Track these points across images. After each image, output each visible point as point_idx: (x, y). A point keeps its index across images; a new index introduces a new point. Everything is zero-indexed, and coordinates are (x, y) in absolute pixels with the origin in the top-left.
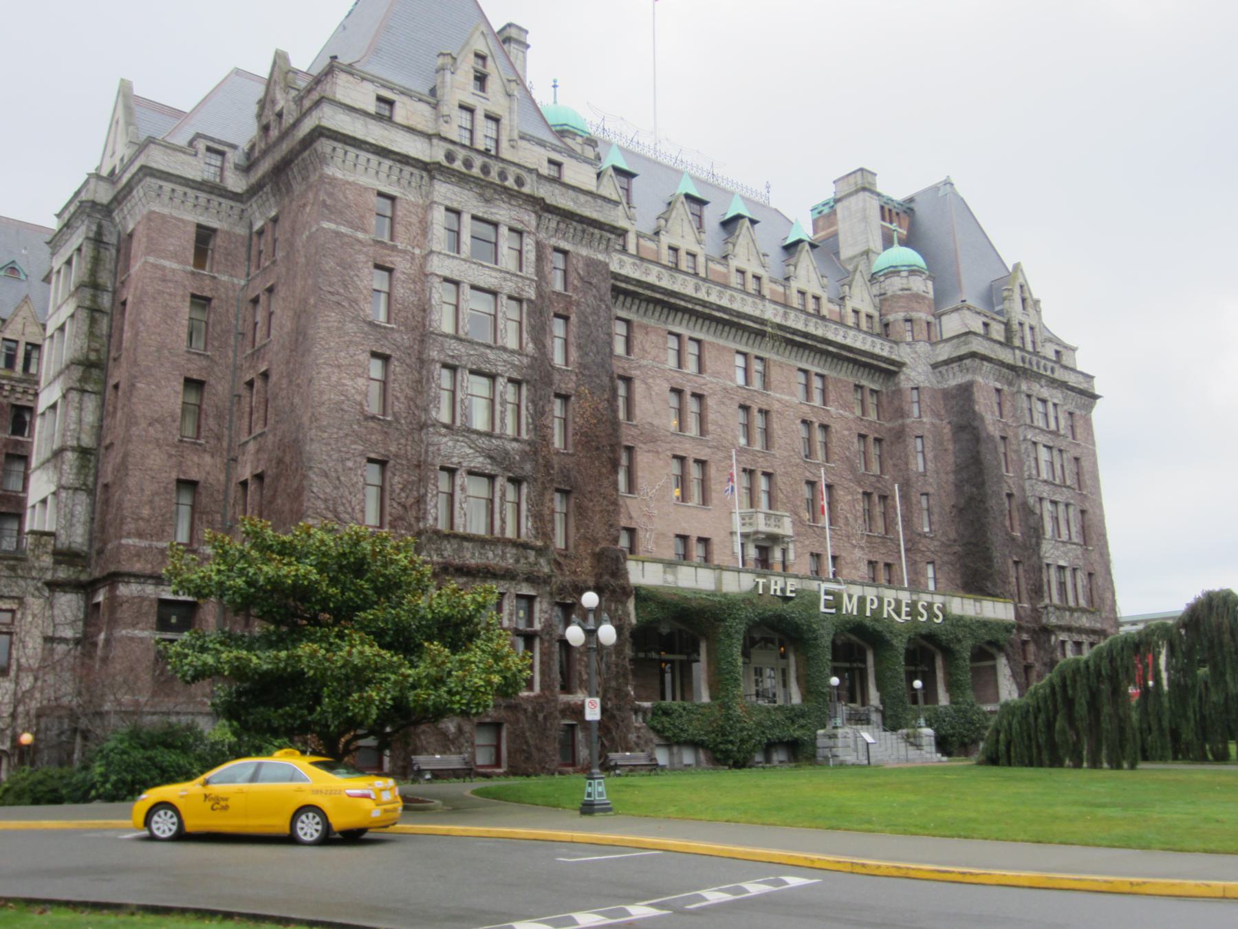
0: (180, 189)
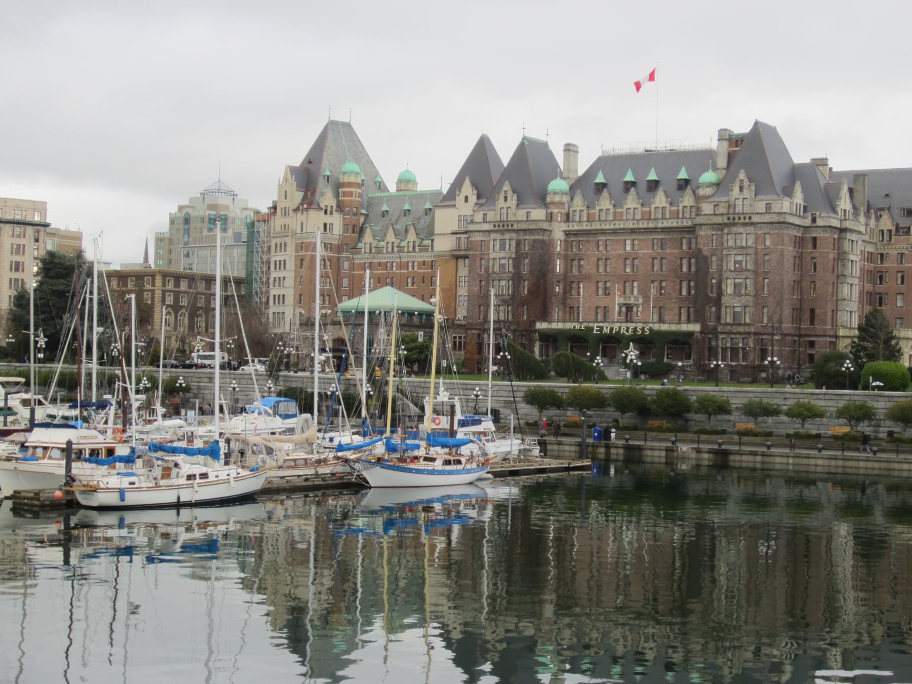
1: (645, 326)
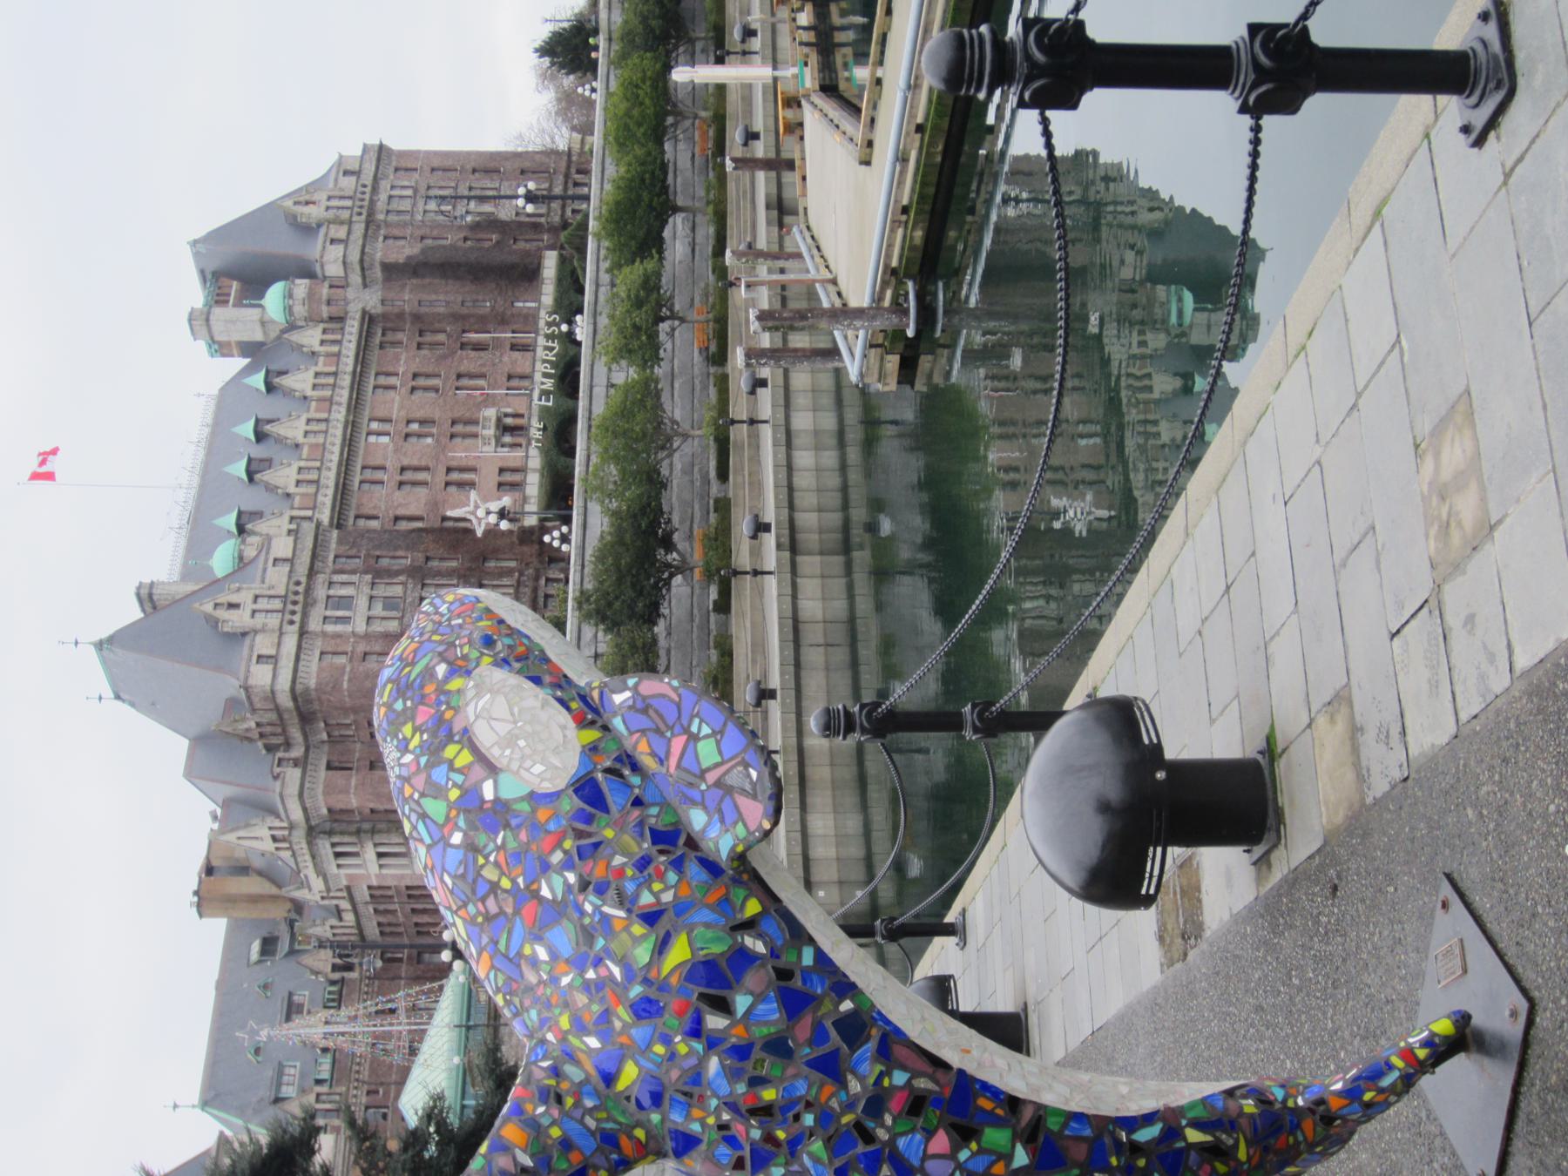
0: (308, 779)
1: (542, 332)
